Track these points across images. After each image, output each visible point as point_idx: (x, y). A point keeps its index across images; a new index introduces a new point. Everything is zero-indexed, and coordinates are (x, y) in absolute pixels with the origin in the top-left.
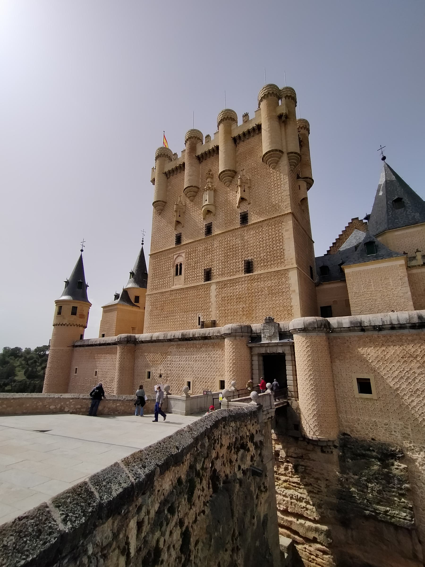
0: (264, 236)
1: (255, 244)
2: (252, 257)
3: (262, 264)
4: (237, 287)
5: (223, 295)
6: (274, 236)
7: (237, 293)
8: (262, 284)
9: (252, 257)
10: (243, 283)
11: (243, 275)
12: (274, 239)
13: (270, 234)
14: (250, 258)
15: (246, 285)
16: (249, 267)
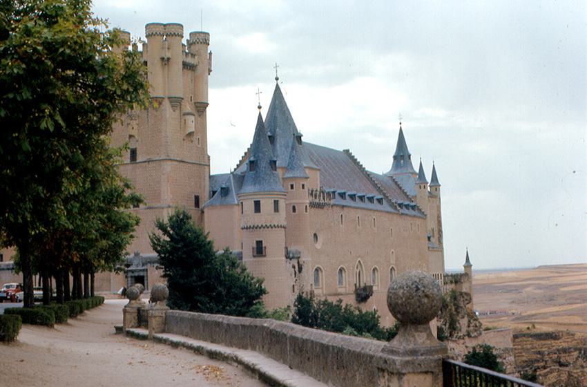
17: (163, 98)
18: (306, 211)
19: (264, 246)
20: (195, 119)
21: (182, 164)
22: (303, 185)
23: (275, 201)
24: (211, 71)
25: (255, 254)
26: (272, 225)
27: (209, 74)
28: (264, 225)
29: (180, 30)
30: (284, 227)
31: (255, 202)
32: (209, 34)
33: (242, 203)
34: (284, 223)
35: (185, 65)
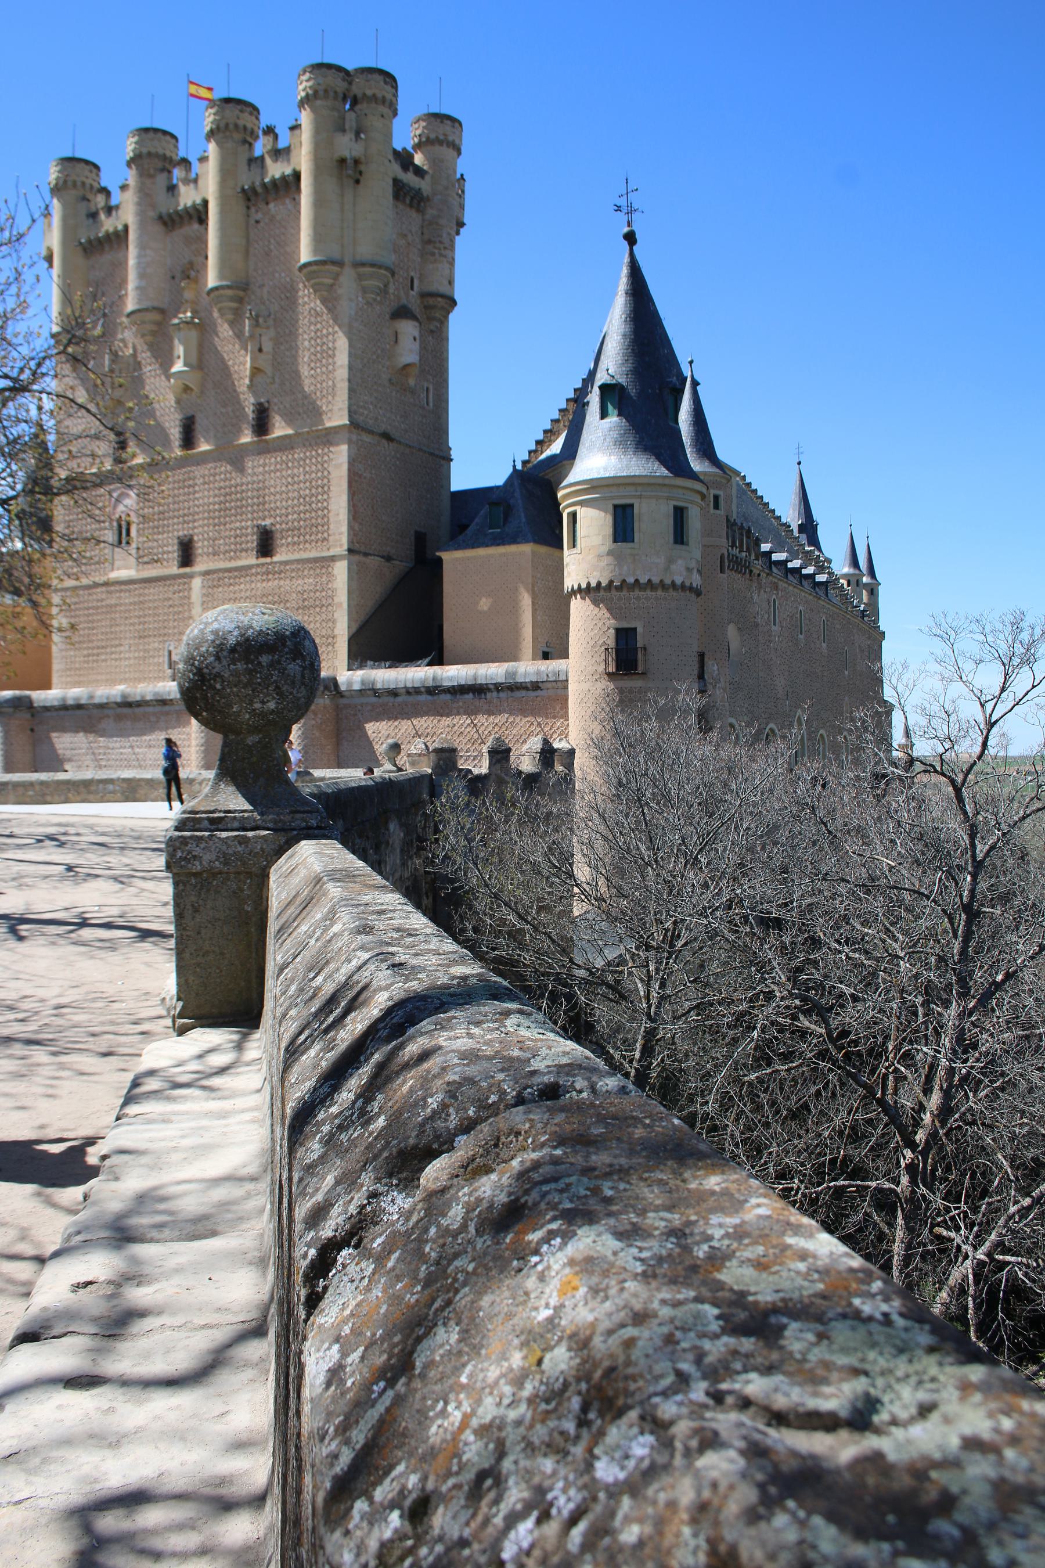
11: (253, 561)
14: (267, 522)
16: (266, 545)
17: (340, 264)
18: (722, 571)
19: (639, 645)
20: (421, 336)
21: (384, 442)
22: (716, 498)
23: (676, 508)
24: (461, 224)
25: (611, 669)
26: (668, 581)
27: (458, 233)
28: (643, 580)
29: (388, 88)
30: (698, 593)
31: (615, 507)
32: (461, 125)
33: (573, 516)
34: (696, 580)
35: (400, 190)
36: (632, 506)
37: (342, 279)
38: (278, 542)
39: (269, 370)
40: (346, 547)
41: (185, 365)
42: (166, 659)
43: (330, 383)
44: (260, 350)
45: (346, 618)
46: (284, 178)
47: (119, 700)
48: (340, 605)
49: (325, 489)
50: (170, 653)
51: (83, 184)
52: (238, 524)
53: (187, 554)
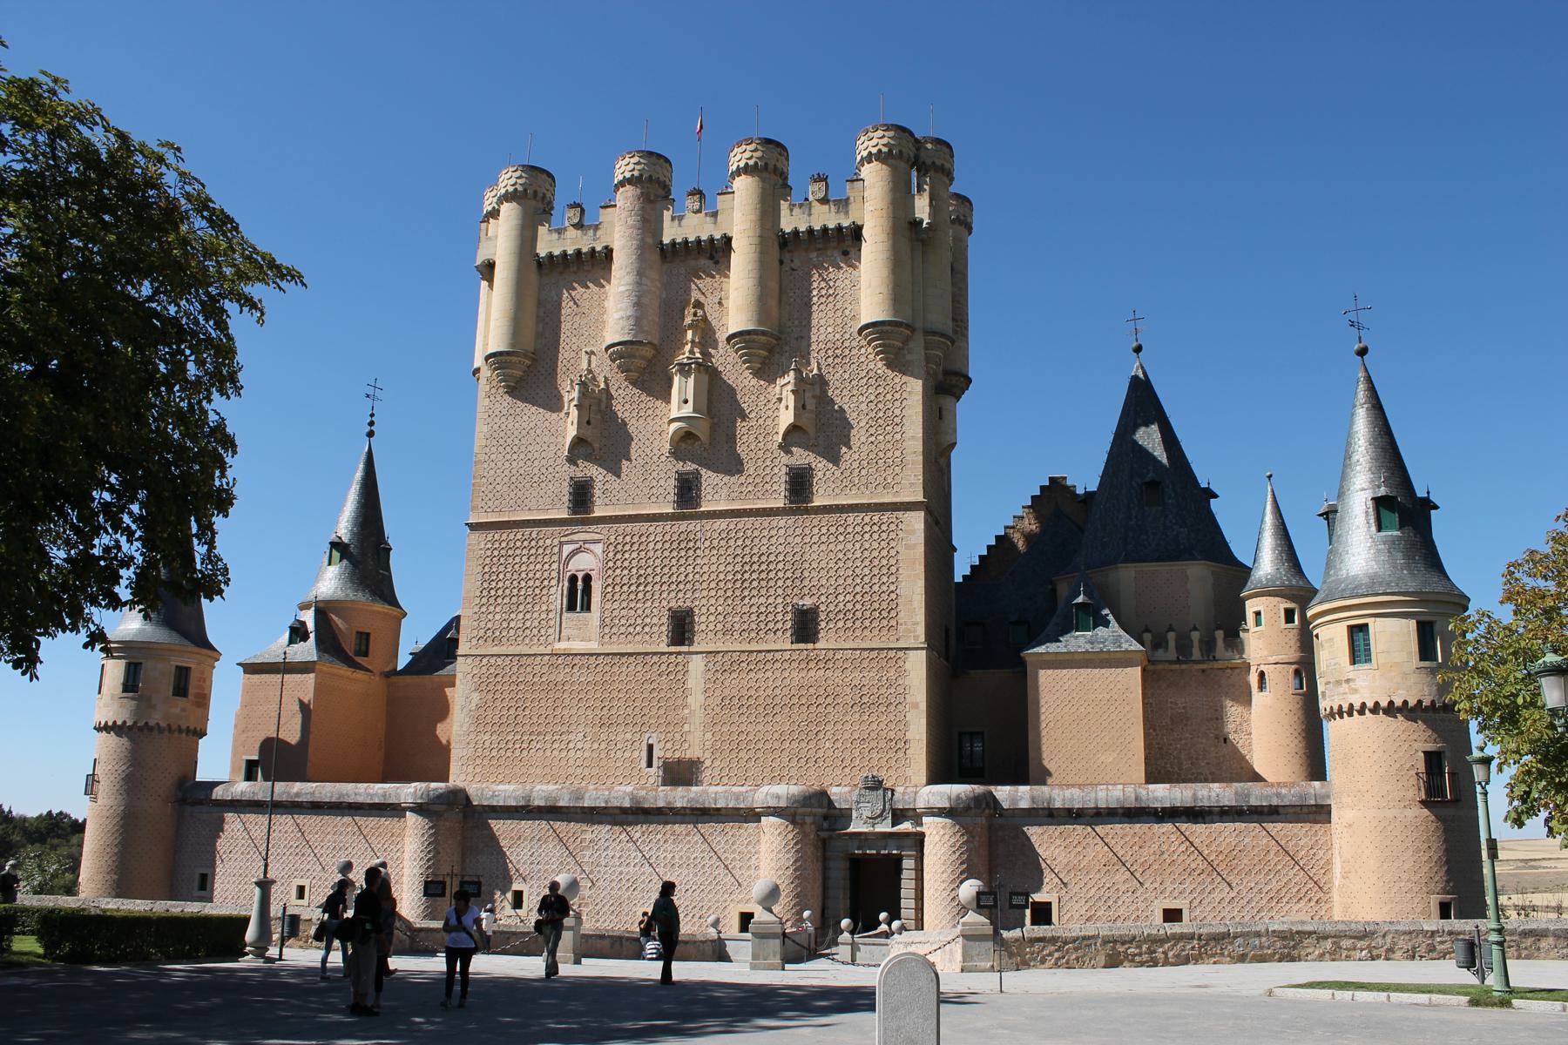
0: (849, 546)
1: (823, 564)
2: (815, 599)
3: (841, 624)
4: (769, 674)
5: (726, 692)
6: (875, 554)
7: (769, 692)
8: (835, 677)
9: (815, 599)
10: (786, 665)
11: (788, 646)
12: (876, 562)
13: (867, 545)
14: (808, 602)
15: (794, 674)
16: (805, 626)
36: (1431, 624)
37: (911, 344)
38: (823, 624)
39: (811, 431)
40: (922, 638)
41: (695, 411)
42: (644, 754)
43: (898, 453)
44: (804, 407)
45: (924, 721)
46: (839, 228)
47: (627, 804)
48: (916, 706)
49: (892, 571)
50: (650, 747)
51: (535, 192)
52: (762, 600)
53: (682, 628)
